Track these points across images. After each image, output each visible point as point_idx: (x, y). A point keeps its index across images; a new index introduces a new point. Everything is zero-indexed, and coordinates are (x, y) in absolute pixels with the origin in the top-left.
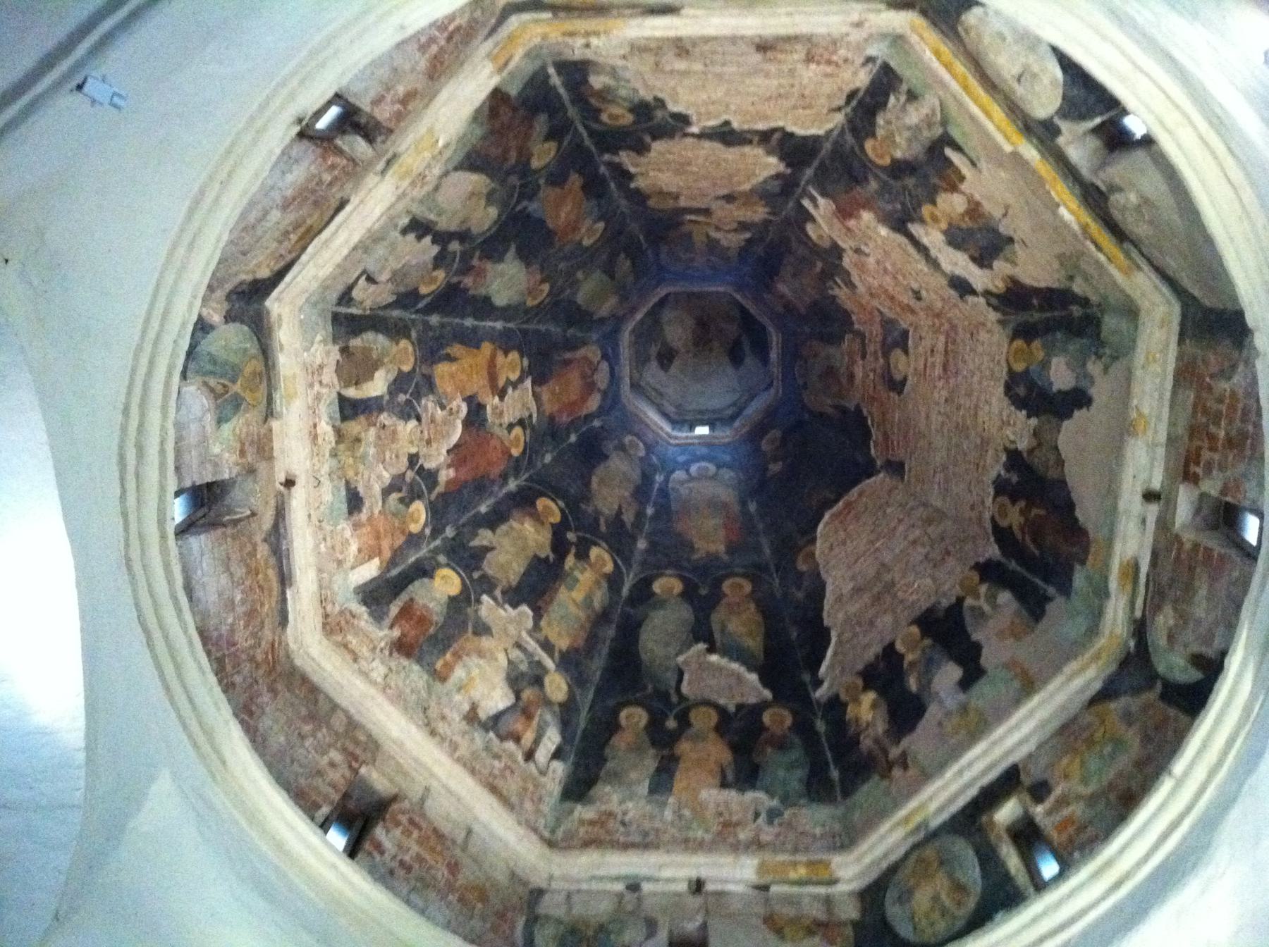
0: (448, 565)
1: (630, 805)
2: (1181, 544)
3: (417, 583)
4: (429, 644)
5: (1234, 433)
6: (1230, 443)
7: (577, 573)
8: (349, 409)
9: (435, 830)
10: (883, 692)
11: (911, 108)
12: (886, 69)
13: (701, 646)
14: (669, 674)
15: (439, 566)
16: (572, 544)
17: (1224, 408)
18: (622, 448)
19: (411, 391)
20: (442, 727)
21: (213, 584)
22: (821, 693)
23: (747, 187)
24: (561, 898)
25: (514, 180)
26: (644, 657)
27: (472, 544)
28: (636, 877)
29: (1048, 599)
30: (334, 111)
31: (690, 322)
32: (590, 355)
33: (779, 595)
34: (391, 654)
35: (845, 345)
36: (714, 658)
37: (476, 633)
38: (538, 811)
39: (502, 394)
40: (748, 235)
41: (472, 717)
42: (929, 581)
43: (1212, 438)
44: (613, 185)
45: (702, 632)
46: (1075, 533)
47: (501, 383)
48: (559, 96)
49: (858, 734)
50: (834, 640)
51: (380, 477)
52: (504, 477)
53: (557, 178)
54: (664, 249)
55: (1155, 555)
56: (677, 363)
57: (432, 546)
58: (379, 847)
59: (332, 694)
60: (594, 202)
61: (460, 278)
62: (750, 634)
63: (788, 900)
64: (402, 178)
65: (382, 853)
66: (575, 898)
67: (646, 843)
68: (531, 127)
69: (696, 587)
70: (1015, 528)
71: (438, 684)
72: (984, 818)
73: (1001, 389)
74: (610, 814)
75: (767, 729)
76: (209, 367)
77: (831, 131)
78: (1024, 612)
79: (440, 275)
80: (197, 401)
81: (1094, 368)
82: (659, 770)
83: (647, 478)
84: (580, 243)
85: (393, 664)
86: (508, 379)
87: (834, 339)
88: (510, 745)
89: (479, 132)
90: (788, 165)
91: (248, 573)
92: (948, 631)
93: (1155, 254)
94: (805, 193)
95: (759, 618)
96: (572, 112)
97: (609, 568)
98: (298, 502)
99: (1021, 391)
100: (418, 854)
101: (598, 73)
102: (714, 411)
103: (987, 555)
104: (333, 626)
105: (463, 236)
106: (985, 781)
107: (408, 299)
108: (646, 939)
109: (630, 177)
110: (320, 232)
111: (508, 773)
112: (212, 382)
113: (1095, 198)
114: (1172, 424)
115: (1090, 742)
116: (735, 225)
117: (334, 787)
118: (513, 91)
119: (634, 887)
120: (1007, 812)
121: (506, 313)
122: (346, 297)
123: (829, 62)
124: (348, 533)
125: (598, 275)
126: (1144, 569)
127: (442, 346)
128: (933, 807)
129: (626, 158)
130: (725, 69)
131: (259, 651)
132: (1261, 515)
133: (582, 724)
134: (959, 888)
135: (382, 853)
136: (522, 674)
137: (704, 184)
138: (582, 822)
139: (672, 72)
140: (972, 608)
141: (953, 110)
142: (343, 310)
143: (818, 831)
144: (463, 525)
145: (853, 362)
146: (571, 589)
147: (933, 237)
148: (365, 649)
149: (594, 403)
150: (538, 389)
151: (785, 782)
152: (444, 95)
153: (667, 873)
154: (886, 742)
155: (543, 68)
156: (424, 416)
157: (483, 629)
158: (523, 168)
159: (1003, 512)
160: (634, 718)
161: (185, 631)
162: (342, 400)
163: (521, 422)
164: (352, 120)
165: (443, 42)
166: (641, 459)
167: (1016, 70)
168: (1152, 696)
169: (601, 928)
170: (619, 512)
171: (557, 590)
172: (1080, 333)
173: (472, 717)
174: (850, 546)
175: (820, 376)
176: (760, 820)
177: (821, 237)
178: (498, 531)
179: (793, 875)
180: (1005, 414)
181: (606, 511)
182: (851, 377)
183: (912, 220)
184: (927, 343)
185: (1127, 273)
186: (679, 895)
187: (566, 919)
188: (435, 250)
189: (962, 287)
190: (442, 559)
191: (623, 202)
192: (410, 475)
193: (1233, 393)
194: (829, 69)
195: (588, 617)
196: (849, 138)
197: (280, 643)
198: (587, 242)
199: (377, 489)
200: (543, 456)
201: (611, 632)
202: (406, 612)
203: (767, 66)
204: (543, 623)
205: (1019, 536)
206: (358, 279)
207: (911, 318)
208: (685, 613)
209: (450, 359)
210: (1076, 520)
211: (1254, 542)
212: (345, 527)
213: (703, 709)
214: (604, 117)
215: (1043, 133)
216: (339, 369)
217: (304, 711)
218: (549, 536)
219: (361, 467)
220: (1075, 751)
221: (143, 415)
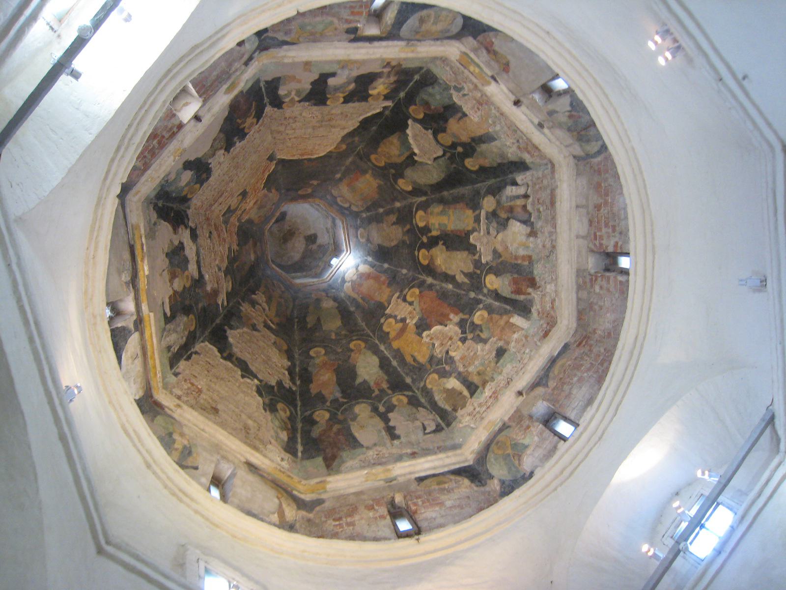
0: (485, 286)
1: (508, 144)
3: (504, 295)
4: (523, 274)
7: (437, 226)
8: (473, 389)
10: (366, 91)
13: (416, 158)
14: (441, 163)
15: (489, 290)
16: (428, 238)
19: (442, 365)
20: (548, 245)
22: (389, 104)
23: (245, 329)
25: (340, 417)
26: (443, 176)
27: (468, 282)
28: (537, 128)
29: (267, 82)
31: (289, 245)
34: (539, 287)
35: (247, 217)
36: (416, 151)
37: (500, 256)
38: (544, 176)
39: (403, 320)
40: (253, 296)
41: (533, 234)
42: (304, 114)
43: (159, 143)
44: (297, 370)
45: (411, 161)
47: (400, 325)
48: (302, 438)
49: (392, 84)
51: (482, 350)
52: (431, 287)
56: (309, 233)
57: (484, 299)
58: (616, 245)
59: (575, 303)
60: (309, 369)
61: (387, 390)
63: (488, 65)
64: (389, 470)
65: (617, 243)
69: (393, 175)
71: (533, 258)
73: (211, 179)
74: (519, 148)
75: (425, 113)
76: (513, 469)
77: (202, 342)
78: (281, 82)
79: (394, 400)
82: (484, 142)
84: (325, 354)
85: (543, 283)
86: (396, 323)
88: (529, 208)
89: (344, 454)
90: (225, 331)
91: (564, 383)
95: (382, 145)
96: (300, 426)
97: (421, 213)
98: (522, 383)
100: (606, 227)
101: (283, 441)
104: (551, 323)
105: (375, 410)
110: (434, 475)
111: (541, 201)
112: (517, 462)
116: (257, 306)
118: (319, 460)
119: (541, 126)
120: (373, 30)
121: (376, 351)
122: (438, 429)
123: (192, 384)
124: (513, 344)
126: (225, 87)
127: (414, 367)
128: (397, 49)
129: (287, 383)
131: (586, 351)
134: (422, 21)
135: (617, 243)
136: (498, 223)
137: (261, 343)
138: (532, 156)
140: (298, 97)
142: (443, 425)
143: (448, 69)
144: (464, 290)
146: (446, 225)
147: (192, 268)
148: (547, 299)
150: (386, 304)
151: (441, 94)
153: (523, 117)
155: (302, 459)
158: (333, 418)
159: (252, 125)
161: (605, 394)
162: (472, 394)
163: (405, 300)
165: (344, 519)
170: (394, 224)
171: (452, 231)
173: (533, 234)
175: (265, 207)
176: (465, 93)
178: (453, 274)
179: (477, 70)
180: (217, 168)
182: (255, 203)
184: (220, 208)
188: (390, 415)
189: (194, 236)
190: (485, 291)
191: (296, 356)
194: (193, 380)
195: (449, 208)
196: (198, 335)
197: (575, 341)
199: (487, 347)
200: (405, 275)
201: (445, 193)
202: (518, 292)
203: (215, 396)
204: (470, 228)
206: (429, 433)
208: (408, 172)
209: (415, 360)
213: (442, 142)
216: (463, 406)
217: (592, 313)
218: (434, 249)
221: (552, 482)
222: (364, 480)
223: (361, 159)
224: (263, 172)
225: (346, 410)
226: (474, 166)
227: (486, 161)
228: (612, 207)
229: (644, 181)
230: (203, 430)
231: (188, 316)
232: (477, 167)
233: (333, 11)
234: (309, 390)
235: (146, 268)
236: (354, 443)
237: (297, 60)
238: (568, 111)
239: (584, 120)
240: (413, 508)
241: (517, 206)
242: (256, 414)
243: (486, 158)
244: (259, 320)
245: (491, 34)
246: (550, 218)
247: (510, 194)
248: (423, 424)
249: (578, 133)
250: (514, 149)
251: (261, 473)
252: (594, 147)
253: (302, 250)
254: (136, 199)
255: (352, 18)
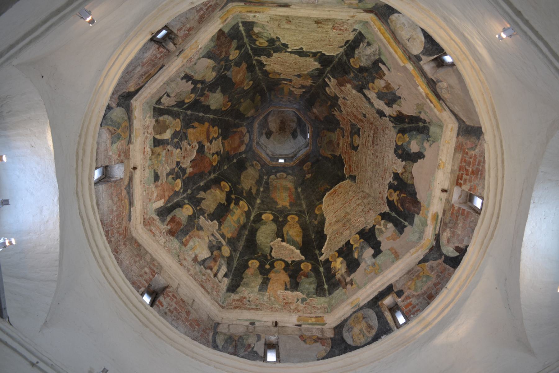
0: (188, 204)
1: (252, 295)
2: (454, 207)
3: (177, 210)
4: (181, 232)
5: (474, 169)
6: (473, 173)
7: (235, 210)
8: (157, 143)
9: (181, 299)
10: (345, 258)
11: (368, 48)
12: (360, 33)
13: (280, 239)
14: (267, 249)
16: (233, 199)
17: (472, 160)
18: (252, 165)
19: (179, 137)
20: (184, 263)
21: (107, 203)
22: (322, 258)
23: (306, 72)
24: (226, 326)
25: (223, 63)
29: (405, 226)
30: (164, 32)
31: (278, 121)
32: (243, 130)
33: (308, 222)
36: (284, 244)
37: (198, 229)
39: (211, 142)
40: (304, 90)
41: (195, 260)
42: (363, 219)
44: (257, 68)
45: (280, 234)
46: (416, 203)
47: (211, 138)
48: (242, 34)
49: (336, 273)
50: (328, 239)
51: (166, 169)
52: (210, 173)
53: (238, 64)
54: (273, 93)
55: (444, 212)
56: (272, 137)
57: (183, 196)
58: (161, 304)
59: (146, 247)
62: (297, 236)
64: (185, 58)
65: (162, 306)
66: (231, 326)
67: (257, 308)
68: (231, 44)
69: (278, 218)
70: (395, 201)
71: (183, 247)
72: (380, 303)
73: (393, 151)
74: (245, 298)
75: (302, 270)
76: (110, 123)
77: (338, 54)
78: (397, 232)
79: (193, 96)
80: (106, 135)
81: (426, 145)
83: (261, 177)
85: (167, 238)
87: (333, 131)
88: (209, 271)
89: (213, 44)
90: (321, 66)
92: (369, 236)
93: (451, 105)
94: (327, 76)
95: (300, 230)
96: (246, 40)
97: (246, 209)
98: (137, 176)
99: (400, 152)
100: (175, 308)
101: (257, 27)
102: (286, 155)
103: (384, 211)
104: (147, 223)
105: (202, 82)
106: (380, 290)
107: (180, 104)
108: (257, 341)
109: (264, 65)
111: (208, 281)
113: (432, 84)
114: (453, 166)
115: (418, 276)
116: (299, 86)
117: (146, 281)
118: (226, 30)
119: (253, 324)
120: (388, 301)
121: (215, 112)
122: (159, 102)
123: (340, 30)
124: (153, 189)
125: (249, 101)
126: (440, 216)
127: (191, 123)
128: (361, 298)
129: (263, 59)
130: (303, 29)
131: (120, 229)
132: (482, 198)
133: (235, 266)
135: (162, 306)
136: (214, 245)
137: (291, 70)
138: (234, 300)
139: (284, 29)
140: (378, 229)
141: (383, 50)
142: (157, 106)
143: (319, 306)
144: (194, 189)
145: (339, 139)
146: (232, 216)
147: (372, 95)
148: (158, 232)
149: (243, 148)
150: (224, 141)
151: (308, 289)
152: (203, 29)
153: (265, 319)
154: (345, 276)
155: (238, 23)
156: (183, 148)
157: (200, 228)
158: (227, 59)
159: (391, 194)
160: (254, 264)
161: (96, 220)
162: (155, 139)
163: (217, 153)
164: (170, 36)
165: (205, 10)
166: (259, 170)
167: (408, 37)
168: (441, 261)
169: (241, 337)
171: (227, 216)
172: (422, 133)
173: (195, 260)
174: (335, 206)
176: (299, 302)
177: (331, 92)
179: (310, 322)
181: (246, 188)
182: (338, 144)
183: (365, 89)
184: (367, 134)
185: (440, 111)
186: (269, 327)
187: (228, 334)
188: (192, 86)
189: (381, 114)
190: (186, 201)
191: (260, 74)
192: (176, 169)
193: (475, 156)
194: (340, 32)
195: (238, 226)
196: (345, 57)
198: (245, 88)
199: (165, 173)
201: (246, 233)
202: (173, 220)
203: (319, 29)
204: (221, 228)
205: (396, 203)
207: (362, 124)
208: (274, 227)
209: (193, 127)
210: (417, 199)
211: (479, 207)
212: (153, 186)
213: (279, 262)
214: (257, 43)
215: (416, 60)
217: (136, 253)
219: (160, 165)
220: (413, 279)
221: (86, 138)
222: (199, 41)
223: (300, 211)
224: (350, 166)
225: (221, 69)
226: (251, 263)
227: (250, 274)
228: (183, 321)
229: (187, 355)
230: (329, 11)
231: (360, 67)
232: (250, 265)
233: (422, 298)
234: (246, 62)
235: (422, 90)
236: (209, 55)
237: (409, 254)
238: (253, 348)
239: (242, 352)
240: (161, 49)
241: (215, 266)
242: (283, 33)
243: (252, 275)
244: (296, 81)
245: (329, 349)
246: (197, 278)
247: (222, 268)
248: (170, 97)
249: (236, 341)
250: (246, 295)
251: (276, 5)
252: (220, 341)
253: (270, 124)
254: (450, 126)
255: (408, 301)
